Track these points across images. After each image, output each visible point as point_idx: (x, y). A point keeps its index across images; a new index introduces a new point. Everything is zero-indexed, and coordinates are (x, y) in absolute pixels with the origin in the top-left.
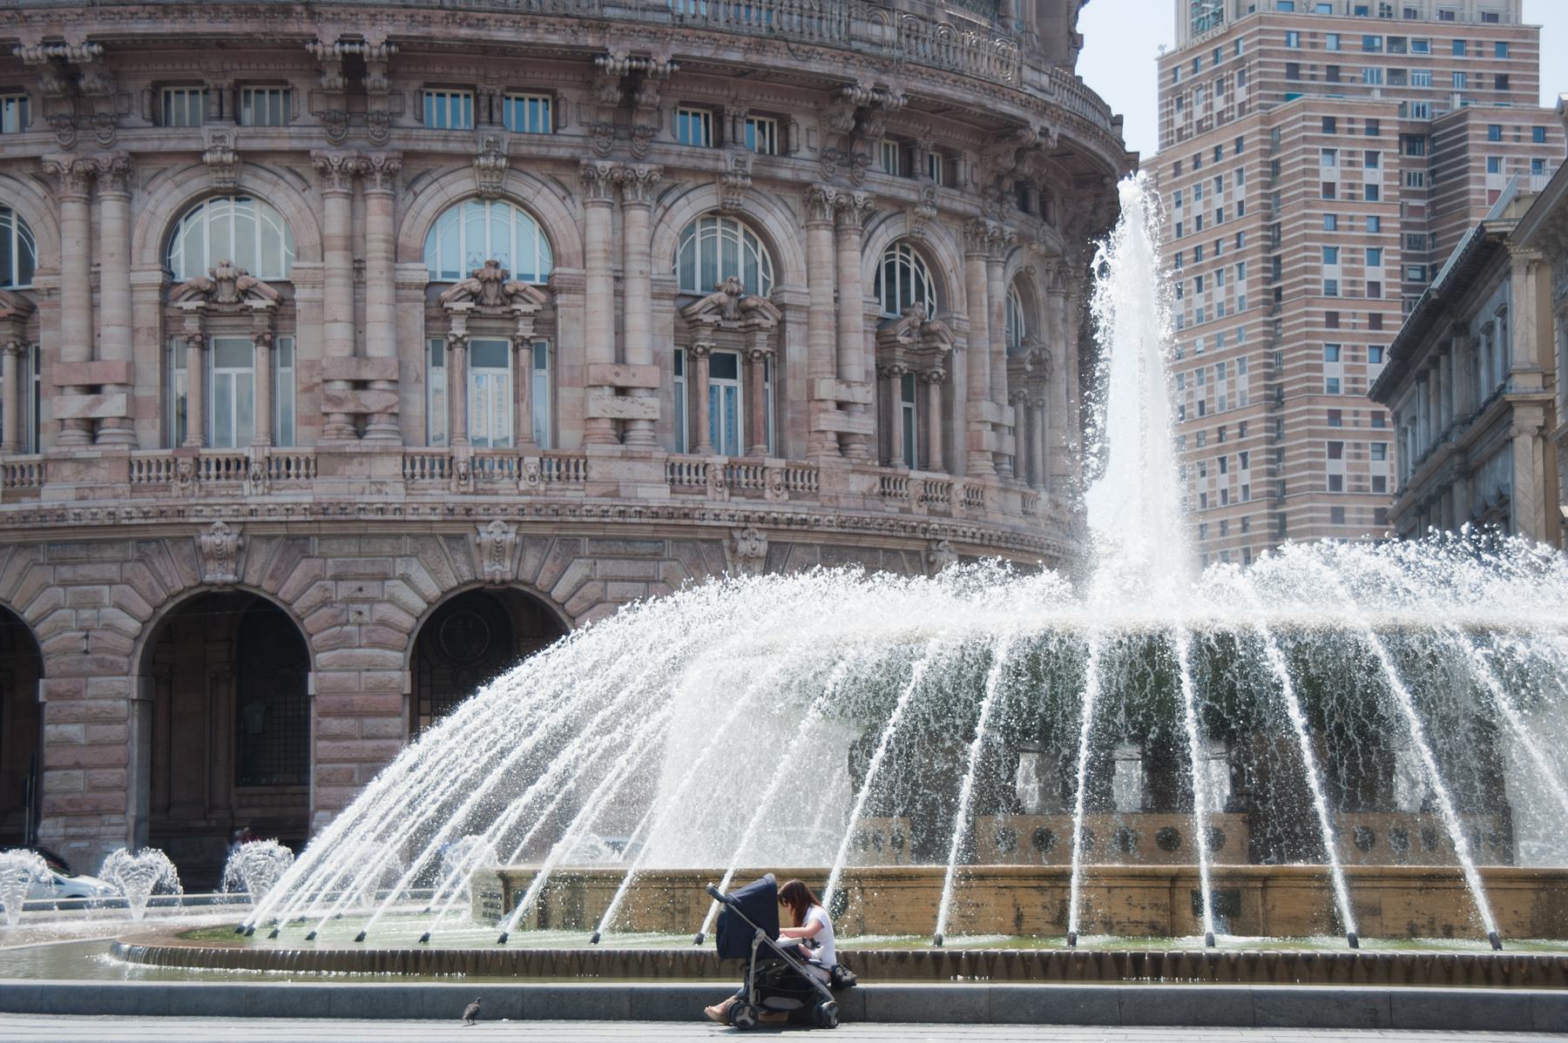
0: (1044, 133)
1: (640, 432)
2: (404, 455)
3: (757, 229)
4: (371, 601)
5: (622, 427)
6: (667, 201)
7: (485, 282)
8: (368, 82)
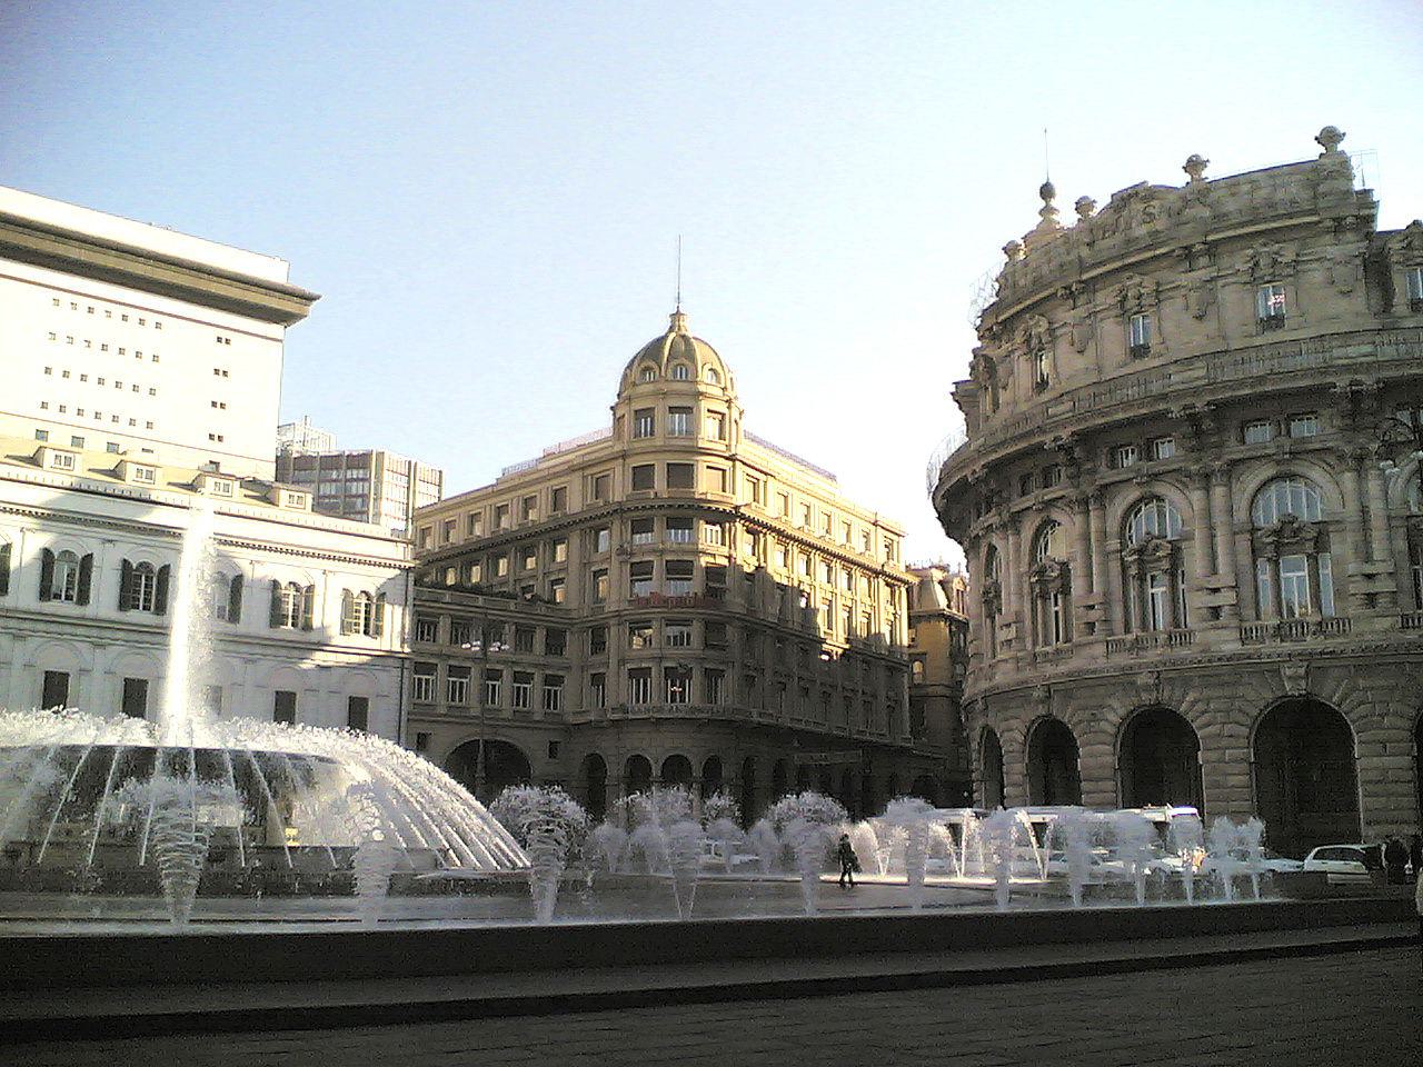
1: (1225, 612)
2: (1107, 642)
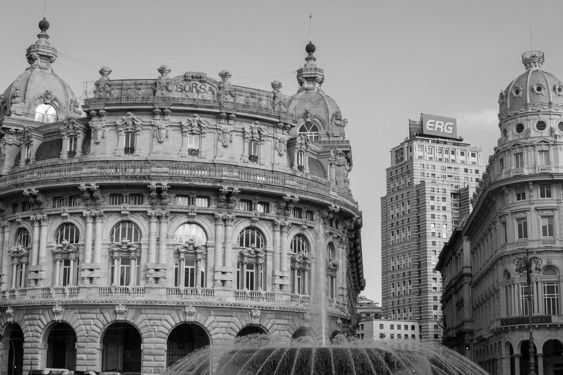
0: (336, 207)
3: (260, 232)
4: (158, 326)
6: (237, 224)
7: (189, 244)
8: (162, 194)
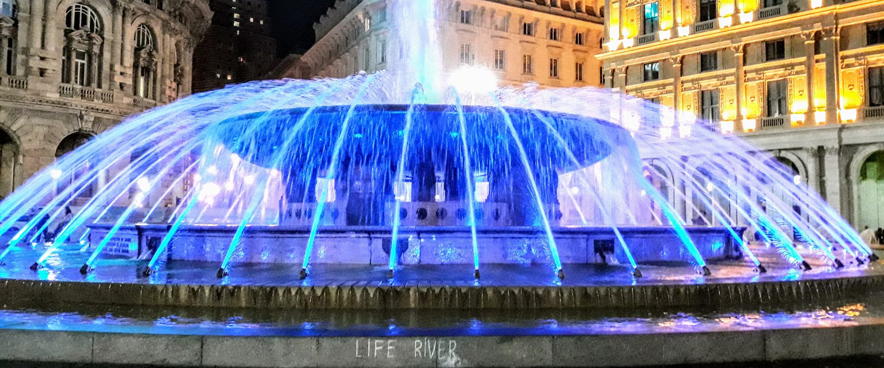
5: (42, 72)
